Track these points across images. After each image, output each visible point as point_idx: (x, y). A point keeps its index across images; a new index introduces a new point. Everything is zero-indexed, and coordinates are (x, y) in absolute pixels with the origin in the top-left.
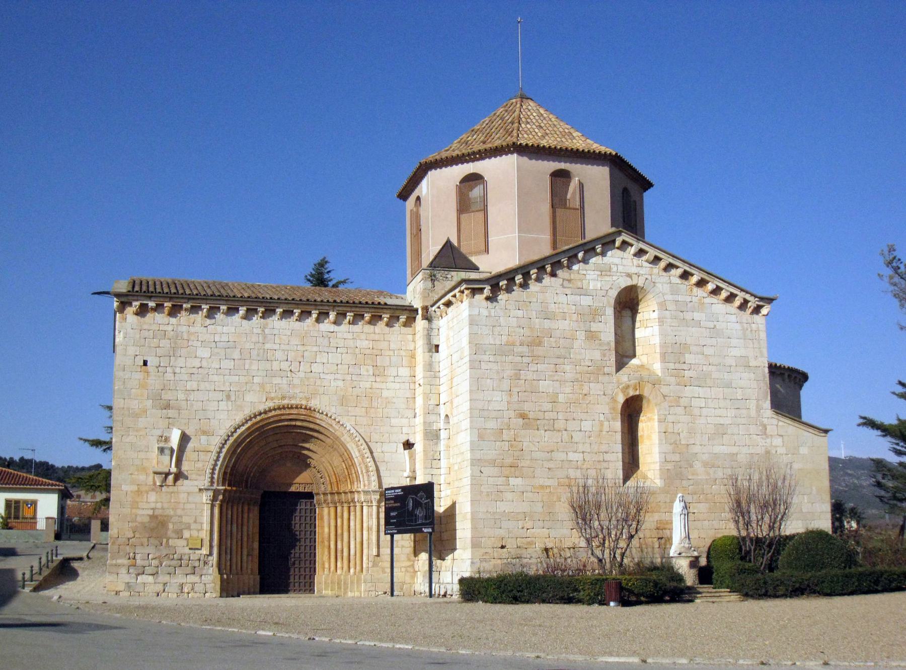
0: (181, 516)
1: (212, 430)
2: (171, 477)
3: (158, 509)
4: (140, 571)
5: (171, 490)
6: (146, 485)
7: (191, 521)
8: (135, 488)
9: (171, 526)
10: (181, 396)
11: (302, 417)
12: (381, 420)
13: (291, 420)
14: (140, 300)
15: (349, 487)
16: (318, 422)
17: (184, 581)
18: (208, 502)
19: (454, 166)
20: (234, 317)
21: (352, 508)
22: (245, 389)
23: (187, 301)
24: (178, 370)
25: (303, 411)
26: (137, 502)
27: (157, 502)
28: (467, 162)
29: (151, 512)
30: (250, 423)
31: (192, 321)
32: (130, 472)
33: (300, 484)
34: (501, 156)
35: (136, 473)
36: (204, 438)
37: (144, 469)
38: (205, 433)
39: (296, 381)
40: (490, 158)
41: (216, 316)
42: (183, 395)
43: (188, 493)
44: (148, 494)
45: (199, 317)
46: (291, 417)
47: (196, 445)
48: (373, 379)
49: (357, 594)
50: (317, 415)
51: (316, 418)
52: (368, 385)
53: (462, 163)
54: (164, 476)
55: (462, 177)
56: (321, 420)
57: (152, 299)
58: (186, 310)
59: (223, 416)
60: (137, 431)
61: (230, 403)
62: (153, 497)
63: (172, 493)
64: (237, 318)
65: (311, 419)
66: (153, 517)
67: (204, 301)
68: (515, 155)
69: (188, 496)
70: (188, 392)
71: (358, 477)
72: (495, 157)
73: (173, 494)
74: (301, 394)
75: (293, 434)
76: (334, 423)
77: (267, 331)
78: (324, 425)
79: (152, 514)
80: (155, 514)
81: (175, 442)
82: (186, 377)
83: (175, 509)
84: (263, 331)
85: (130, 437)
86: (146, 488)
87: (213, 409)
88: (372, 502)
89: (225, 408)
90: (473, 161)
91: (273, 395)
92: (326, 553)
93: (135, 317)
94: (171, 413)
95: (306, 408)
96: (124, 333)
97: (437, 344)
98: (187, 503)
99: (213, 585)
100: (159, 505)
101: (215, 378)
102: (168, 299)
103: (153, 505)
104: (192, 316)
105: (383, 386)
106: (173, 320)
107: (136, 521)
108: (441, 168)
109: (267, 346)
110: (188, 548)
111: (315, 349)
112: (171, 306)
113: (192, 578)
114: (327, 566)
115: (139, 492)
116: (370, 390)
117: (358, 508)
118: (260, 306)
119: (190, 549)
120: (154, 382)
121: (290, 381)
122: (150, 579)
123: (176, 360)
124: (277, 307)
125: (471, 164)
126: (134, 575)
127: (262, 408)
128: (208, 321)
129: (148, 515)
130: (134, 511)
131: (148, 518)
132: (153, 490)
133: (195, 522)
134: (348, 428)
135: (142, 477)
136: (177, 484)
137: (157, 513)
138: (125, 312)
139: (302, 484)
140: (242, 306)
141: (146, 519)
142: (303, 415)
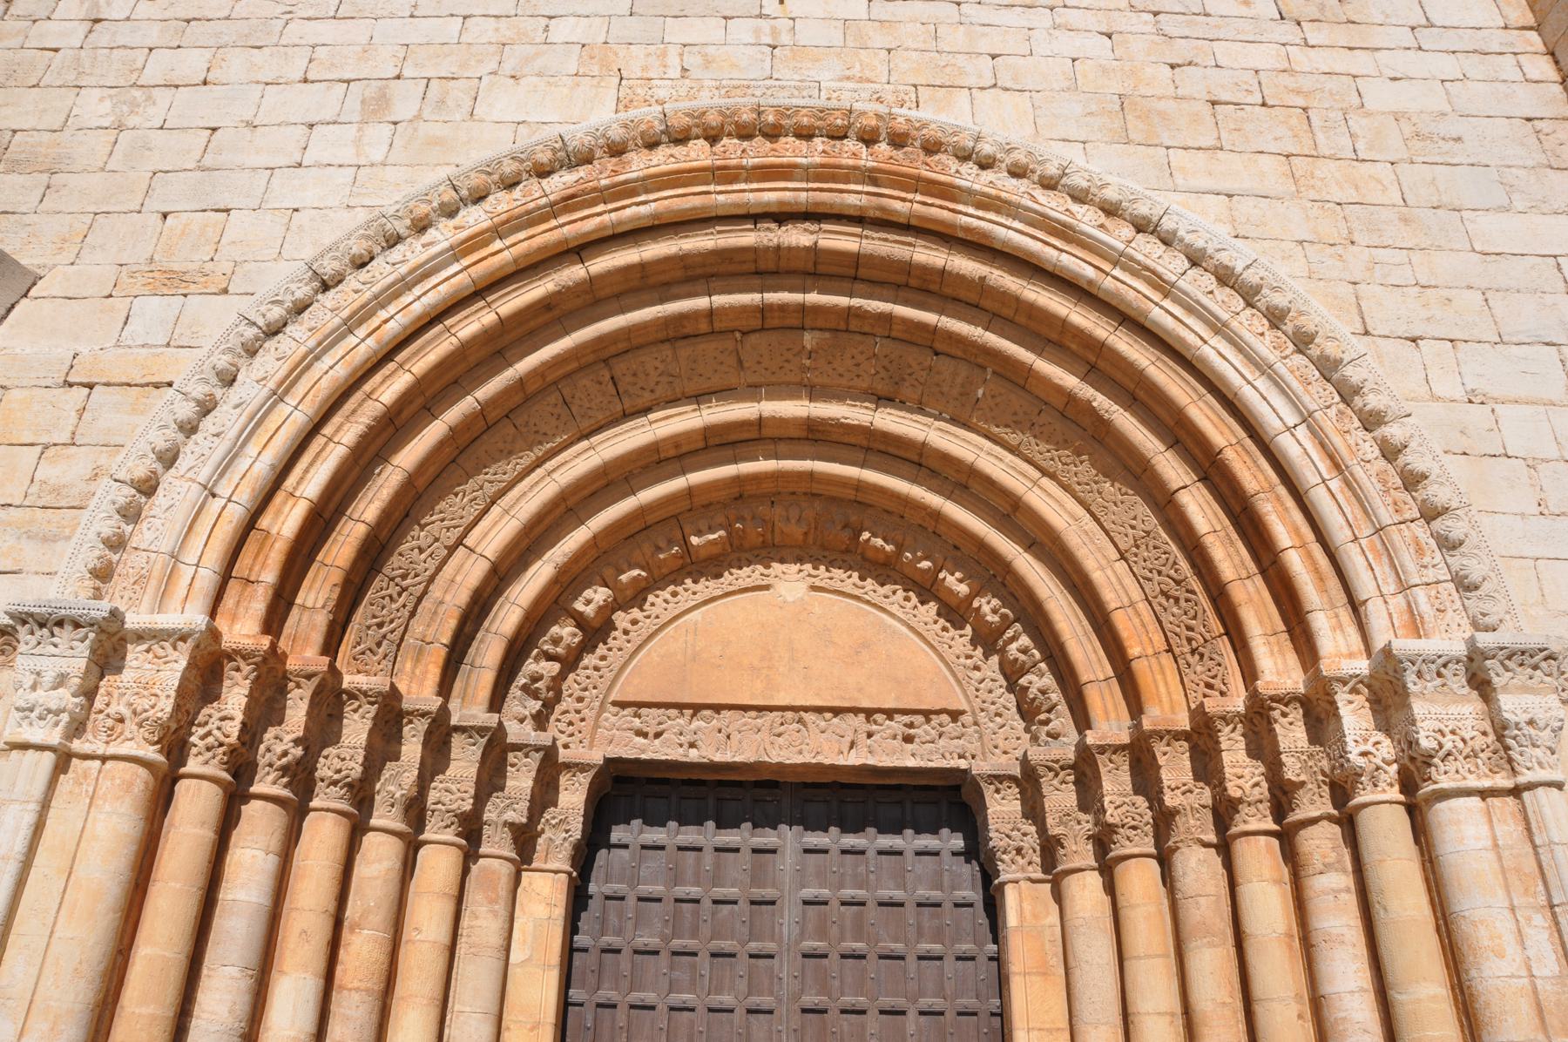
1: (227, 267)
11: (855, 197)
12: (1405, 220)
13: (782, 216)
16: (969, 218)
22: (493, 66)
30: (475, 218)
33: (869, 713)
36: (153, 312)
38: (174, 282)
42: (107, 106)
46: (771, 195)
47: (84, 350)
48: (1288, 31)
50: (969, 177)
51: (947, 192)
52: (1265, 57)
59: (308, 190)
70: (137, 93)
74: (850, 85)
75: (809, 340)
89: (347, 155)
105: (1360, 63)
116: (1285, 79)
121: (774, 32)
127: (578, 135)
139: (890, 714)
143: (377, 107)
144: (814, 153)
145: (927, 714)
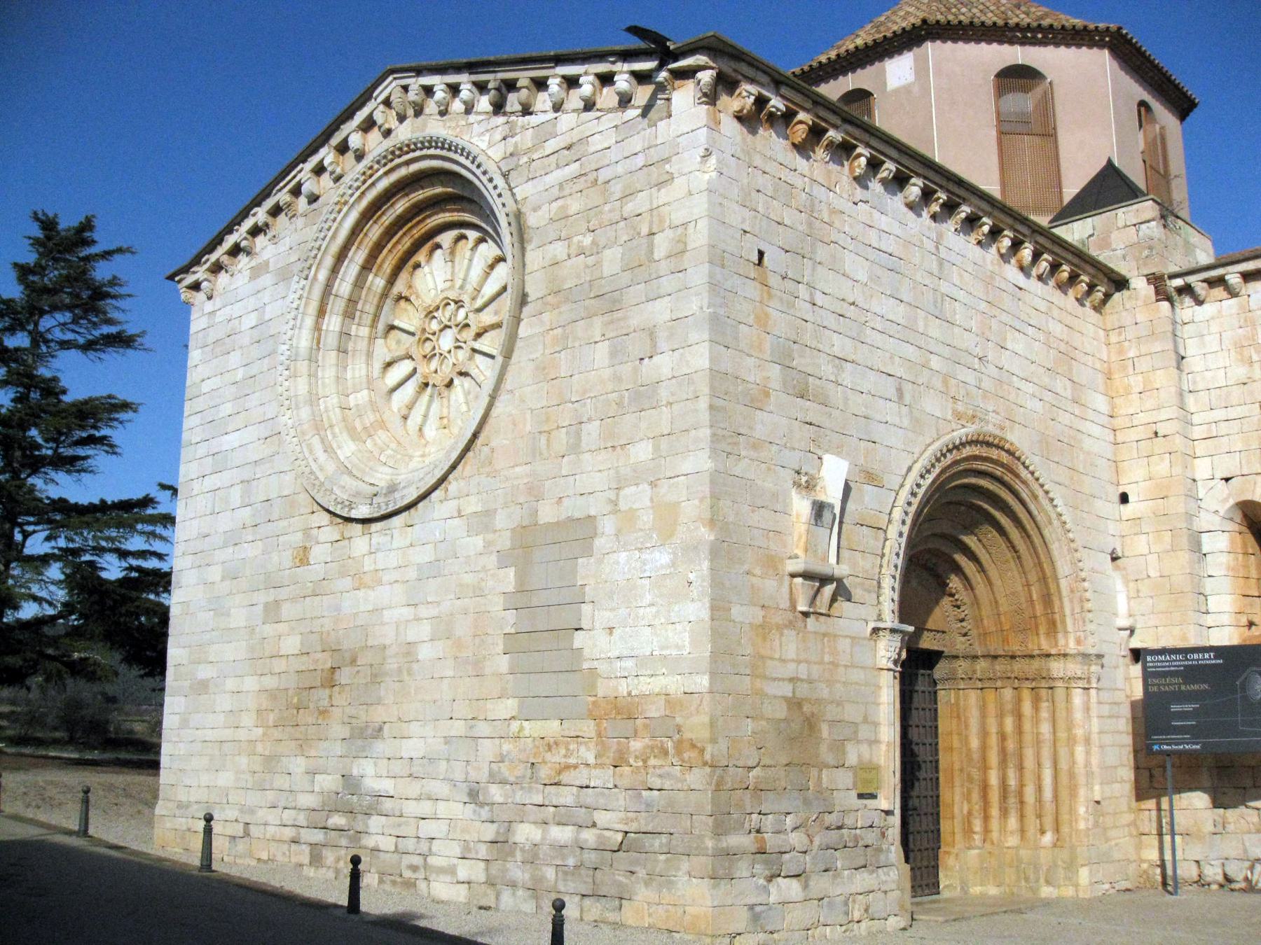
0: (839, 704)
2: (829, 590)
3: (802, 680)
4: (775, 870)
5: (823, 629)
6: (778, 608)
7: (859, 720)
8: (757, 615)
9: (825, 730)
10: (827, 370)
11: (999, 472)
14: (762, 85)
15: (1045, 645)
16: (1019, 487)
17: (854, 889)
18: (891, 666)
19: (983, 45)
20: (894, 198)
21: (1044, 693)
23: (839, 122)
24: (819, 299)
25: (1005, 458)
26: (762, 657)
27: (799, 662)
28: (1011, 42)
29: (786, 690)
31: (834, 179)
32: (746, 567)
34: (1079, 46)
35: (758, 571)
37: (771, 563)
39: (987, 384)
40: (1057, 45)
41: (870, 184)
43: (853, 638)
44: (782, 635)
45: (842, 174)
49: (1069, 892)
50: (1024, 473)
51: (1017, 476)
53: (1001, 42)
54: (817, 584)
55: (1002, 67)
56: (1024, 482)
57: (784, 90)
58: (831, 145)
60: (755, 447)
61: (905, 410)
62: (790, 645)
63: (824, 635)
64: (896, 203)
65: (1008, 478)
66: (795, 704)
67: (866, 137)
68: (1106, 52)
69: (852, 647)
70: (837, 361)
71: (1064, 622)
72: (1068, 45)
73: (826, 639)
75: (963, 508)
76: (1040, 493)
77: (943, 253)
78: (1024, 495)
79: (790, 695)
80: (798, 695)
81: (833, 495)
82: (831, 321)
83: (830, 683)
84: (937, 248)
85: (744, 464)
86: (778, 619)
87: (878, 417)
88: (1089, 682)
90: (1023, 42)
91: (960, 407)
92: (976, 796)
93: (736, 125)
94: (812, 411)
95: (1008, 451)
96: (719, 161)
97: (1183, 355)
98: (853, 666)
99: (898, 892)
100: (803, 671)
101: (877, 338)
102: (809, 105)
103: (790, 670)
104: (833, 167)
106: (800, 162)
107: (762, 718)
108: (955, 40)
109: (944, 287)
110: (854, 794)
111: (1004, 317)
112: (811, 123)
113: (863, 880)
114: (977, 825)
115: (763, 630)
117: (1060, 693)
118: (941, 187)
119: (861, 796)
120: (780, 323)
122: (792, 888)
123: (814, 270)
124: (964, 199)
125: (1018, 48)
126: (762, 881)
128: (859, 193)
129: (785, 698)
130: (758, 683)
131: (785, 706)
132: (791, 625)
133: (865, 720)
134: (1059, 509)
135: (770, 584)
136: (832, 612)
137: (803, 691)
138: (718, 103)
139: (932, 631)
140: (918, 175)
141: (781, 712)
142: (1002, 465)
143: (900, 391)
144: (994, 454)
145: (938, 632)
